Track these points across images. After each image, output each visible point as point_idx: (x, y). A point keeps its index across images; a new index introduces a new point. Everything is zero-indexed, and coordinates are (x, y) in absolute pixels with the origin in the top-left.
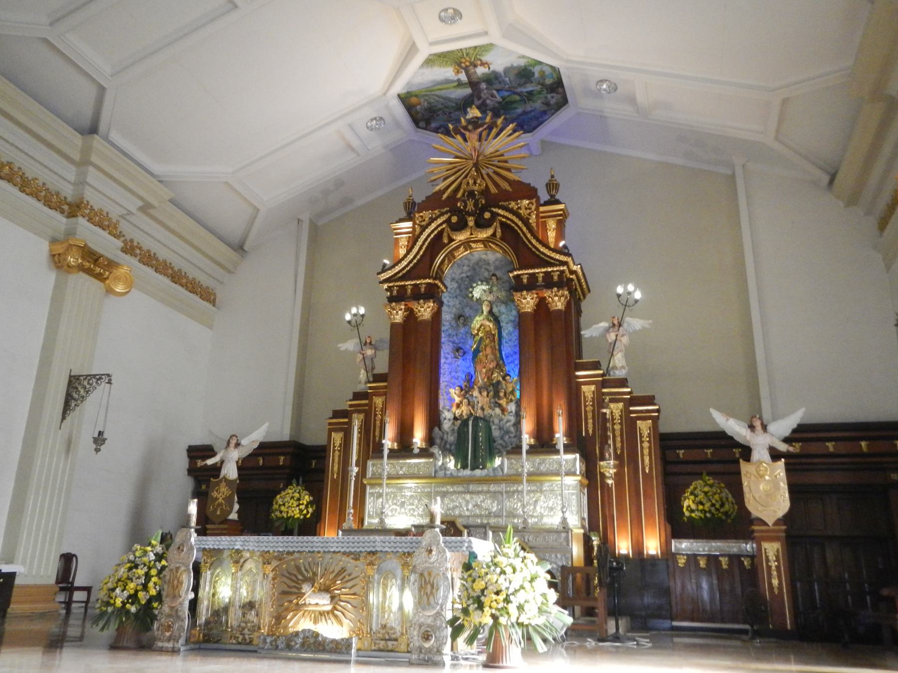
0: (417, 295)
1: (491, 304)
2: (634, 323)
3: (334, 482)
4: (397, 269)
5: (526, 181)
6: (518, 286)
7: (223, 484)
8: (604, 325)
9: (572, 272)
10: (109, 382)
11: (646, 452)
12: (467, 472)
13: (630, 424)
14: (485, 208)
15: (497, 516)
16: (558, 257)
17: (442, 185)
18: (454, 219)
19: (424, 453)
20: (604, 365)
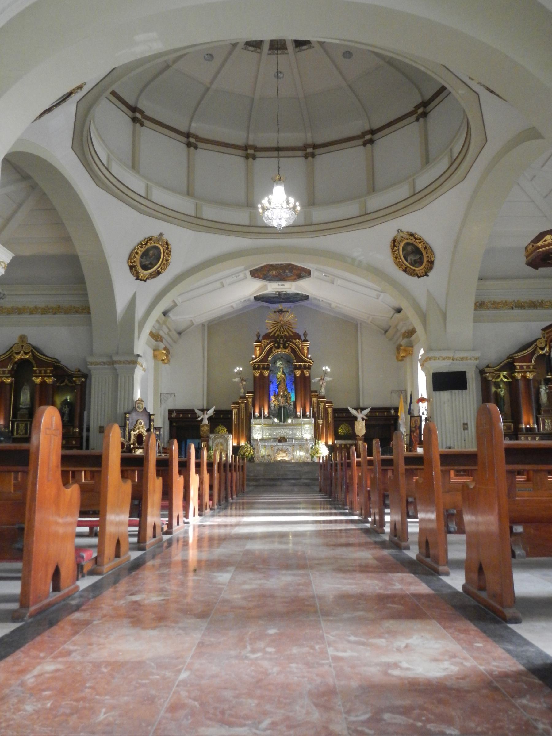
0: (264, 368)
1: (283, 368)
2: (328, 379)
3: (235, 424)
4: (258, 359)
5: (298, 332)
6: (296, 368)
7: (205, 426)
8: (319, 378)
9: (311, 363)
10: (175, 396)
11: (330, 417)
12: (282, 423)
13: (326, 410)
14: (286, 342)
15: (289, 435)
16: (308, 360)
17: (270, 331)
18: (276, 345)
19: (269, 417)
20: (318, 392)
